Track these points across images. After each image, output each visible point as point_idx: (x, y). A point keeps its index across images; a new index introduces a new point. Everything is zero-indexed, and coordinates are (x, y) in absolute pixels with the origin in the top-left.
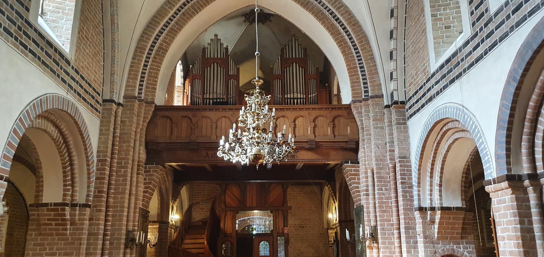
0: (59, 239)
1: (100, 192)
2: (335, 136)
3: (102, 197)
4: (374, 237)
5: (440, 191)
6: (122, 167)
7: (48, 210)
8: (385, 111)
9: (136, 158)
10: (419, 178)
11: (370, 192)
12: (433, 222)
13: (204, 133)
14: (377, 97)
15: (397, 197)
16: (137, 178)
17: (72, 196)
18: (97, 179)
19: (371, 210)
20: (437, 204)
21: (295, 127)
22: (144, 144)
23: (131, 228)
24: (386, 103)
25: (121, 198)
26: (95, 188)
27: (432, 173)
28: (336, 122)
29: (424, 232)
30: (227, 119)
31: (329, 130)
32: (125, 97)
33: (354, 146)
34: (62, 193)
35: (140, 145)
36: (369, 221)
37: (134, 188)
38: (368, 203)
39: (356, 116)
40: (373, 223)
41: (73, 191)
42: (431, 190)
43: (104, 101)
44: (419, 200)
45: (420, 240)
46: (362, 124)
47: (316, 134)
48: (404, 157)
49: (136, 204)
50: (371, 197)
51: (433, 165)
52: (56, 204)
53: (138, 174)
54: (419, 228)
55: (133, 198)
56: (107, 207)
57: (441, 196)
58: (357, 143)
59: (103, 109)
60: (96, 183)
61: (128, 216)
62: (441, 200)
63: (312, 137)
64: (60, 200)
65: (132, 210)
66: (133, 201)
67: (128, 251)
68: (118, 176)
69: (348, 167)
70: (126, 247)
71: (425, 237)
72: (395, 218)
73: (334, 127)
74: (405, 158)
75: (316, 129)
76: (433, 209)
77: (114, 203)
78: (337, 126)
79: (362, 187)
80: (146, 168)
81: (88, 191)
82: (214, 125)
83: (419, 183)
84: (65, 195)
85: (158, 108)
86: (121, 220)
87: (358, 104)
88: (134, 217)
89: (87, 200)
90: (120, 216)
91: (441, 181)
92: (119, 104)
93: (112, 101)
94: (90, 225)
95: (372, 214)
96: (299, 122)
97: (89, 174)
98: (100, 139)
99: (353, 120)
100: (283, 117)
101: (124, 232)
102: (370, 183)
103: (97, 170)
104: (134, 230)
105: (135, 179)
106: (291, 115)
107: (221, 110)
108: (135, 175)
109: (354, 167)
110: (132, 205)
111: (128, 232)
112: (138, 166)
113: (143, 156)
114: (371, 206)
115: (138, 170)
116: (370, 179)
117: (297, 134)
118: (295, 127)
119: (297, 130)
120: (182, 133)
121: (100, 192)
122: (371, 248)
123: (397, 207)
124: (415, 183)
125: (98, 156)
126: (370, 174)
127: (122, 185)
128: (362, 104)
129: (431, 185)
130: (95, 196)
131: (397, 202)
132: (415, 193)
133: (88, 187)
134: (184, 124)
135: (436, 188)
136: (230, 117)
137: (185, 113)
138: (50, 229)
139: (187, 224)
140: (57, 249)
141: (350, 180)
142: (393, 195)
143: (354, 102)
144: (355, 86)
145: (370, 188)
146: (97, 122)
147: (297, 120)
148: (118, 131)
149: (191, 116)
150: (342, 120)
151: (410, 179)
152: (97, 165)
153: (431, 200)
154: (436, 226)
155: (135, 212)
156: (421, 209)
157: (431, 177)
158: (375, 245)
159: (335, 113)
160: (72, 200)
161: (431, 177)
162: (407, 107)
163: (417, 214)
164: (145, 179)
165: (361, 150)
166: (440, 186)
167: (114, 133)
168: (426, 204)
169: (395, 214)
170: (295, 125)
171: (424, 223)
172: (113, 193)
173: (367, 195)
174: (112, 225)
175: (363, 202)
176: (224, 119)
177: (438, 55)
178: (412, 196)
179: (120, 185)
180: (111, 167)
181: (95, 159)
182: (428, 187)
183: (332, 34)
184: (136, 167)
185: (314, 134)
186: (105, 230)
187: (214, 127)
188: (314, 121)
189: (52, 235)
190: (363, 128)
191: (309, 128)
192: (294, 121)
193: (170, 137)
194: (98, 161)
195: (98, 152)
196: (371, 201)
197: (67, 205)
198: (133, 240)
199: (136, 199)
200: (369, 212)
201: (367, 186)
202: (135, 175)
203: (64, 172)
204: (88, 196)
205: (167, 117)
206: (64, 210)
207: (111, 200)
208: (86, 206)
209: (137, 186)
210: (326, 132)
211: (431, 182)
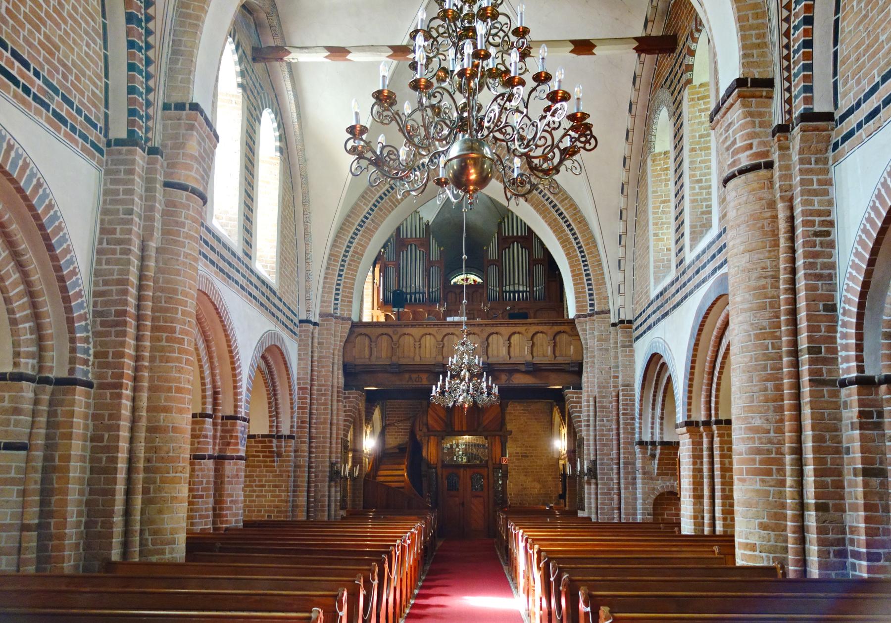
0: (267, 471)
1: (302, 422)
3: (305, 427)
4: (593, 472)
5: (661, 424)
6: (322, 395)
7: (256, 442)
8: (612, 329)
9: (335, 384)
10: (641, 410)
11: (592, 423)
12: (653, 456)
13: (406, 353)
14: (603, 312)
15: (618, 429)
16: (338, 406)
17: (277, 427)
18: (299, 408)
19: (592, 442)
20: (657, 438)
21: (509, 347)
22: (341, 367)
23: (334, 460)
24: (612, 321)
25: (324, 428)
26: (298, 418)
27: (654, 405)
28: (558, 338)
29: (643, 468)
31: (550, 349)
32: (321, 315)
33: (577, 369)
34: (268, 424)
35: (338, 369)
36: (589, 454)
37: (335, 417)
38: (588, 435)
39: (580, 334)
40: (592, 458)
41: (277, 422)
42: (653, 423)
43: (301, 321)
44: (640, 433)
45: (639, 476)
46: (587, 344)
47: (535, 354)
48: (628, 385)
49: (337, 434)
50: (591, 428)
51: (654, 396)
52: (263, 436)
53: (338, 401)
54: (639, 464)
55: (334, 427)
56: (310, 438)
57: (662, 429)
58: (581, 365)
59: (300, 331)
60: (298, 413)
61: (330, 447)
62: (662, 433)
63: (529, 358)
64: (266, 432)
65: (334, 441)
66: (334, 432)
67: (333, 484)
68: (318, 404)
69: (570, 393)
70: (331, 479)
71: (644, 473)
72: (615, 452)
73: (555, 346)
74: (629, 386)
75: (535, 349)
76: (653, 443)
77: (317, 433)
78: (558, 345)
79: (584, 417)
80: (345, 394)
81: (292, 422)
82: (417, 344)
83: (641, 415)
84: (271, 427)
85: (354, 325)
86: (324, 452)
87: (582, 319)
88: (337, 448)
89: (292, 432)
90: (323, 447)
91: (662, 414)
92: (316, 324)
93: (308, 321)
94: (295, 457)
95: (592, 448)
96: (515, 339)
97: (292, 404)
98: (299, 364)
100: (497, 333)
101: (328, 464)
102: (592, 413)
103: (299, 398)
104: (337, 462)
105: (335, 407)
106: (505, 331)
108: (335, 403)
109: (577, 393)
110: (334, 436)
111: (332, 465)
112: (338, 392)
113: (342, 381)
114: (592, 438)
115: (338, 396)
116: (592, 409)
117: (512, 354)
118: (509, 347)
119: (512, 349)
120: (382, 354)
121: (302, 422)
122: (589, 483)
123: (618, 440)
124: (637, 415)
125: (299, 384)
126: (592, 403)
127: (324, 414)
128: (587, 319)
129: (653, 418)
130: (298, 427)
131: (618, 435)
132: (637, 425)
133: (292, 417)
134: (384, 342)
135: (658, 421)
137: (385, 330)
138: (258, 461)
139: (382, 458)
140: (266, 481)
141: (572, 407)
142: (614, 427)
143: (578, 316)
144: (579, 297)
145: (592, 418)
146: (296, 346)
147: (512, 338)
148: (316, 354)
149: (391, 333)
150: (564, 338)
151: (633, 410)
152: (298, 394)
153: (652, 433)
154: (656, 462)
155: (337, 443)
156: (641, 443)
157: (653, 409)
158: (593, 481)
159: (557, 328)
160: (278, 432)
161: (653, 409)
162: (634, 327)
163: (637, 449)
164: (345, 407)
165: (584, 375)
166: (662, 418)
167: (312, 357)
168: (647, 438)
169: (615, 447)
170: (510, 343)
171: (643, 458)
172: (315, 423)
173: (588, 426)
174: (316, 457)
175: (584, 433)
176: (428, 336)
177: (657, 280)
178: (633, 429)
179: (320, 414)
180: (311, 395)
181: (296, 387)
182: (650, 420)
183: (554, 232)
184: (335, 394)
185: (532, 353)
186: (310, 462)
187: (417, 346)
188: (532, 339)
189: (260, 467)
190: (587, 349)
192: (509, 339)
193: (369, 359)
194: (299, 389)
195: (298, 379)
196: (592, 433)
197: (273, 436)
198: (338, 473)
199: (338, 429)
200: (588, 445)
201: (589, 416)
202: (335, 403)
203: (269, 403)
204: (292, 427)
206: (271, 442)
207: (313, 430)
208: (291, 437)
209: (338, 415)
210: (544, 353)
211: (653, 414)
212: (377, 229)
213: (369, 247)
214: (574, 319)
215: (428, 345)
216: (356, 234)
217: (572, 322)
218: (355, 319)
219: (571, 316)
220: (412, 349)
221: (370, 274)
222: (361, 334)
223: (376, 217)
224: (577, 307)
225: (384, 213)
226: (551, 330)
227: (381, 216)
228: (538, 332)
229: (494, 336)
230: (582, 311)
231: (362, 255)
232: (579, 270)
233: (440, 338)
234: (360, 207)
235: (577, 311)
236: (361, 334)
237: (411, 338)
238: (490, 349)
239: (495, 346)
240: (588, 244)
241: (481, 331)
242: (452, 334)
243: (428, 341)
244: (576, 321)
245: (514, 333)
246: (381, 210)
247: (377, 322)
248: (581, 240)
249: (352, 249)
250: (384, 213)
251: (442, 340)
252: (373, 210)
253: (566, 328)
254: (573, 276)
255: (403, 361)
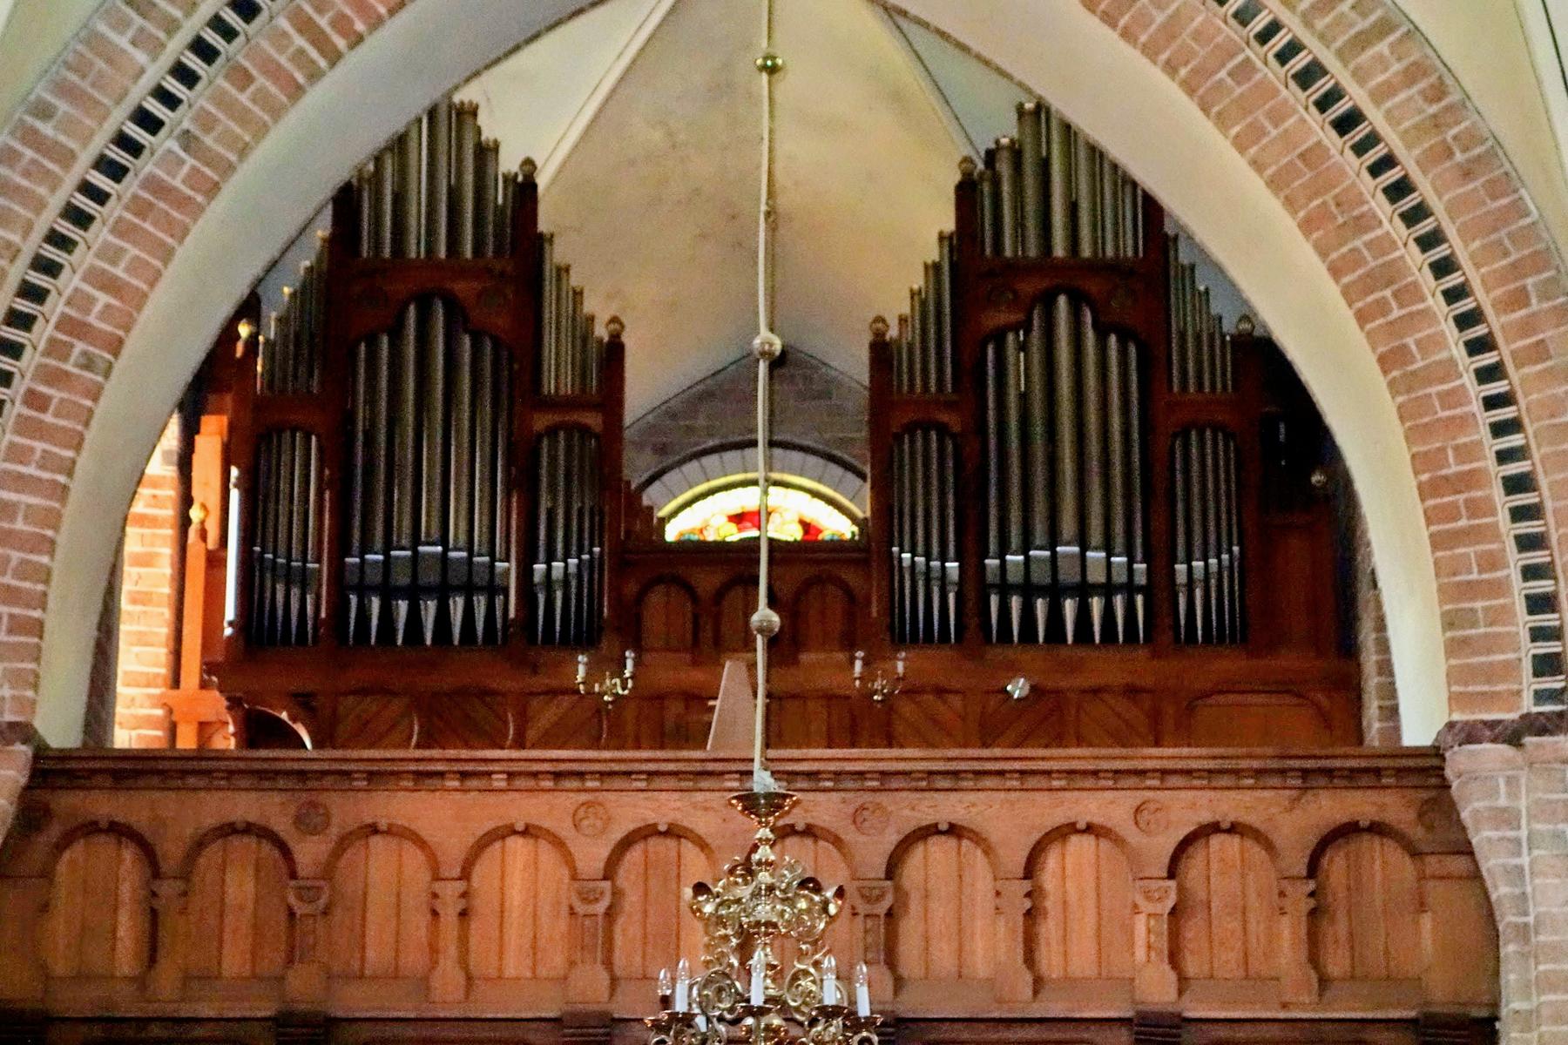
2: (1324, 982)
13: (376, 955)
21: (1032, 916)
30: (544, 845)
47: (1192, 966)
75: (1193, 931)
85: (51, 772)
99: (1458, 864)
100: (954, 831)
106: (1007, 816)
107: (499, 782)
118: (1032, 916)
119: (1049, 929)
136: (565, 830)
147: (1052, 861)
159: (1331, 807)
187: (449, 914)
191: (1140, 924)
192: (1031, 868)
193: (141, 982)
205: (120, 831)
212: (213, 190)
213: (160, 301)
214: (1436, 752)
215: (516, 896)
216: (81, 219)
217: (1426, 771)
218: (60, 729)
219: (1417, 731)
220: (418, 924)
221: (161, 467)
222: (91, 829)
223: (207, 122)
224: (1452, 676)
225: (262, 98)
226: (1296, 818)
227: (243, 117)
228: (1214, 828)
229: (939, 851)
230: (1488, 699)
231: (116, 346)
232: (1465, 453)
233: (592, 854)
234: (112, 56)
235: (1455, 700)
236: (91, 829)
237: (414, 859)
238: (910, 929)
239: (941, 911)
240: (1519, 299)
241: (856, 817)
242: (674, 832)
243: (521, 882)
244: (1459, 761)
245: (1066, 831)
246: (242, 78)
247: (202, 754)
248: (1470, 272)
249: (55, 307)
250: (262, 98)
251: (609, 873)
252: (187, 77)
253: (1392, 806)
254: (1425, 491)
255: (354, 1001)
